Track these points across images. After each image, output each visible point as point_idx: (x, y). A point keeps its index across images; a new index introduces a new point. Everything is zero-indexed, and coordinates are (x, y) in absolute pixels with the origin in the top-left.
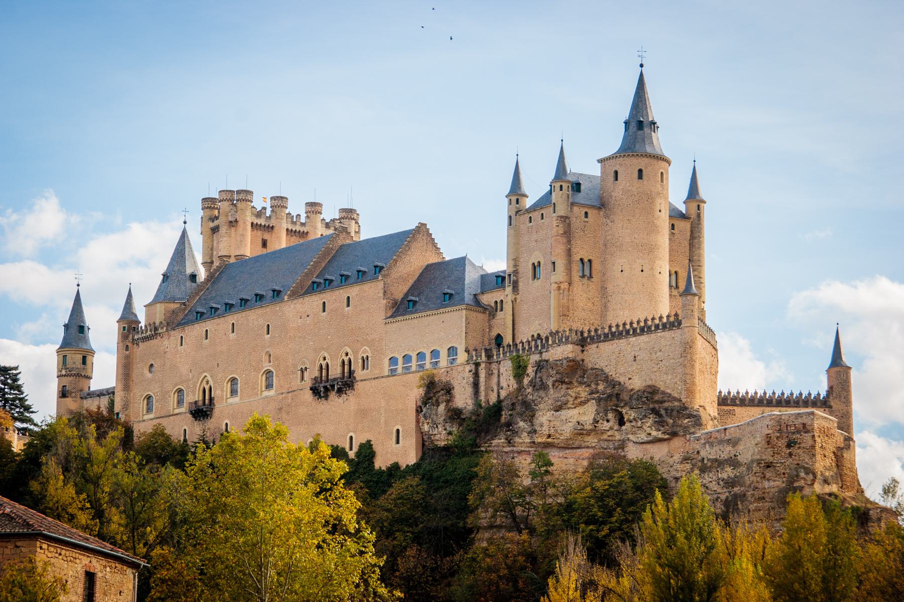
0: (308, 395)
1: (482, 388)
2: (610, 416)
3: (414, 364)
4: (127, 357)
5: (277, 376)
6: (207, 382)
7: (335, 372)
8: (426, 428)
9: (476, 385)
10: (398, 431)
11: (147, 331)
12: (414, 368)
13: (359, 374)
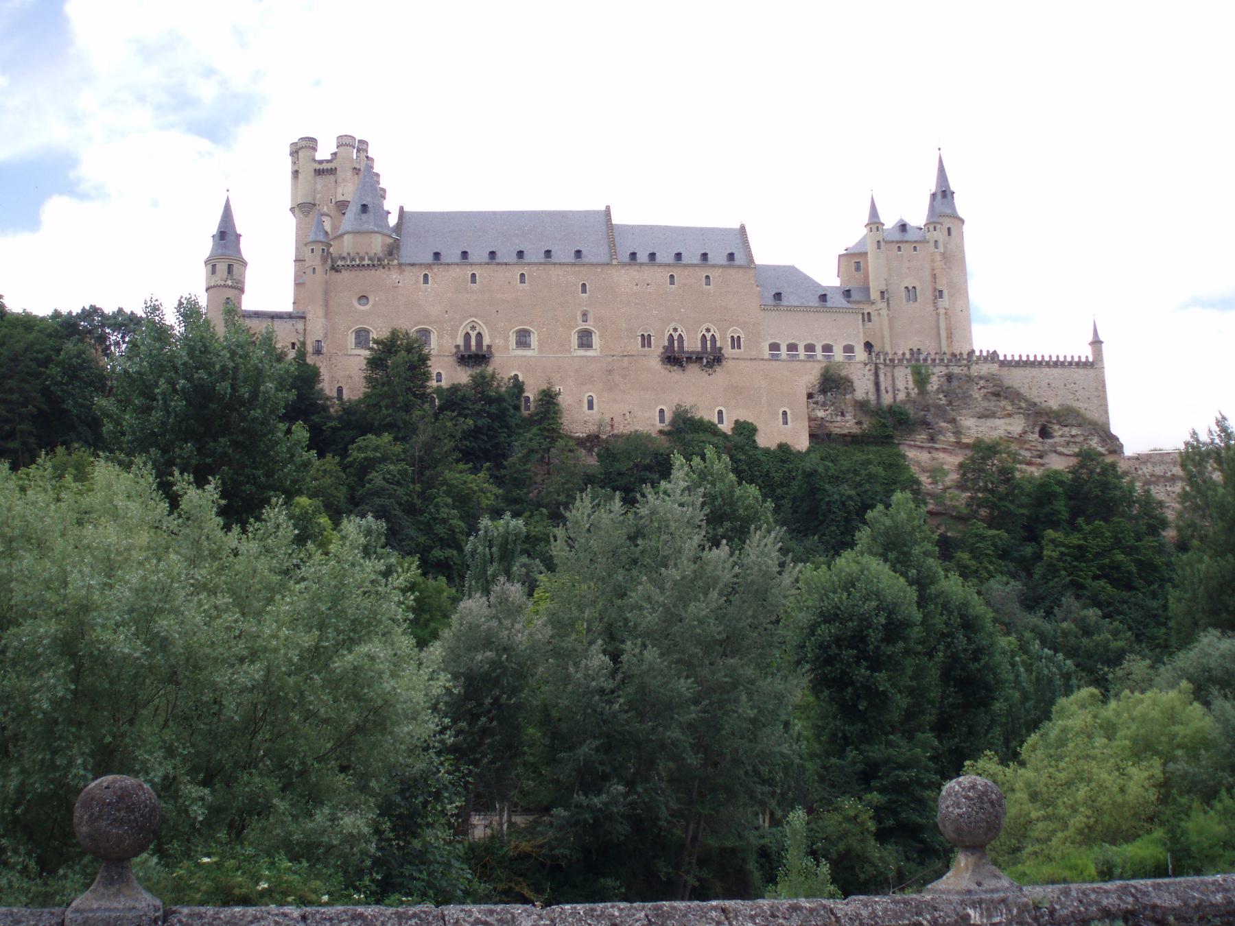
0: (655, 362)
1: (882, 388)
2: (1037, 429)
3: (802, 352)
4: (326, 282)
5: (601, 337)
6: (473, 328)
7: (692, 344)
8: (821, 414)
9: (877, 385)
10: (785, 413)
11: (362, 259)
12: (802, 357)
13: (728, 351)
